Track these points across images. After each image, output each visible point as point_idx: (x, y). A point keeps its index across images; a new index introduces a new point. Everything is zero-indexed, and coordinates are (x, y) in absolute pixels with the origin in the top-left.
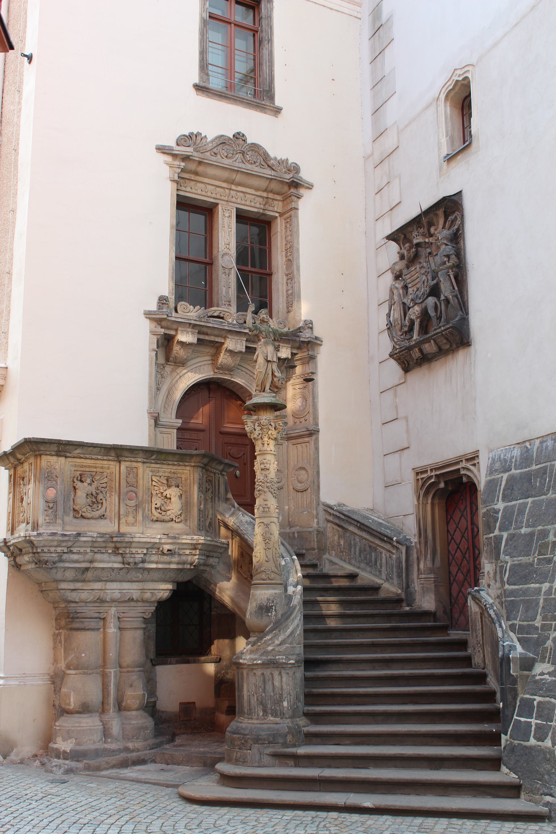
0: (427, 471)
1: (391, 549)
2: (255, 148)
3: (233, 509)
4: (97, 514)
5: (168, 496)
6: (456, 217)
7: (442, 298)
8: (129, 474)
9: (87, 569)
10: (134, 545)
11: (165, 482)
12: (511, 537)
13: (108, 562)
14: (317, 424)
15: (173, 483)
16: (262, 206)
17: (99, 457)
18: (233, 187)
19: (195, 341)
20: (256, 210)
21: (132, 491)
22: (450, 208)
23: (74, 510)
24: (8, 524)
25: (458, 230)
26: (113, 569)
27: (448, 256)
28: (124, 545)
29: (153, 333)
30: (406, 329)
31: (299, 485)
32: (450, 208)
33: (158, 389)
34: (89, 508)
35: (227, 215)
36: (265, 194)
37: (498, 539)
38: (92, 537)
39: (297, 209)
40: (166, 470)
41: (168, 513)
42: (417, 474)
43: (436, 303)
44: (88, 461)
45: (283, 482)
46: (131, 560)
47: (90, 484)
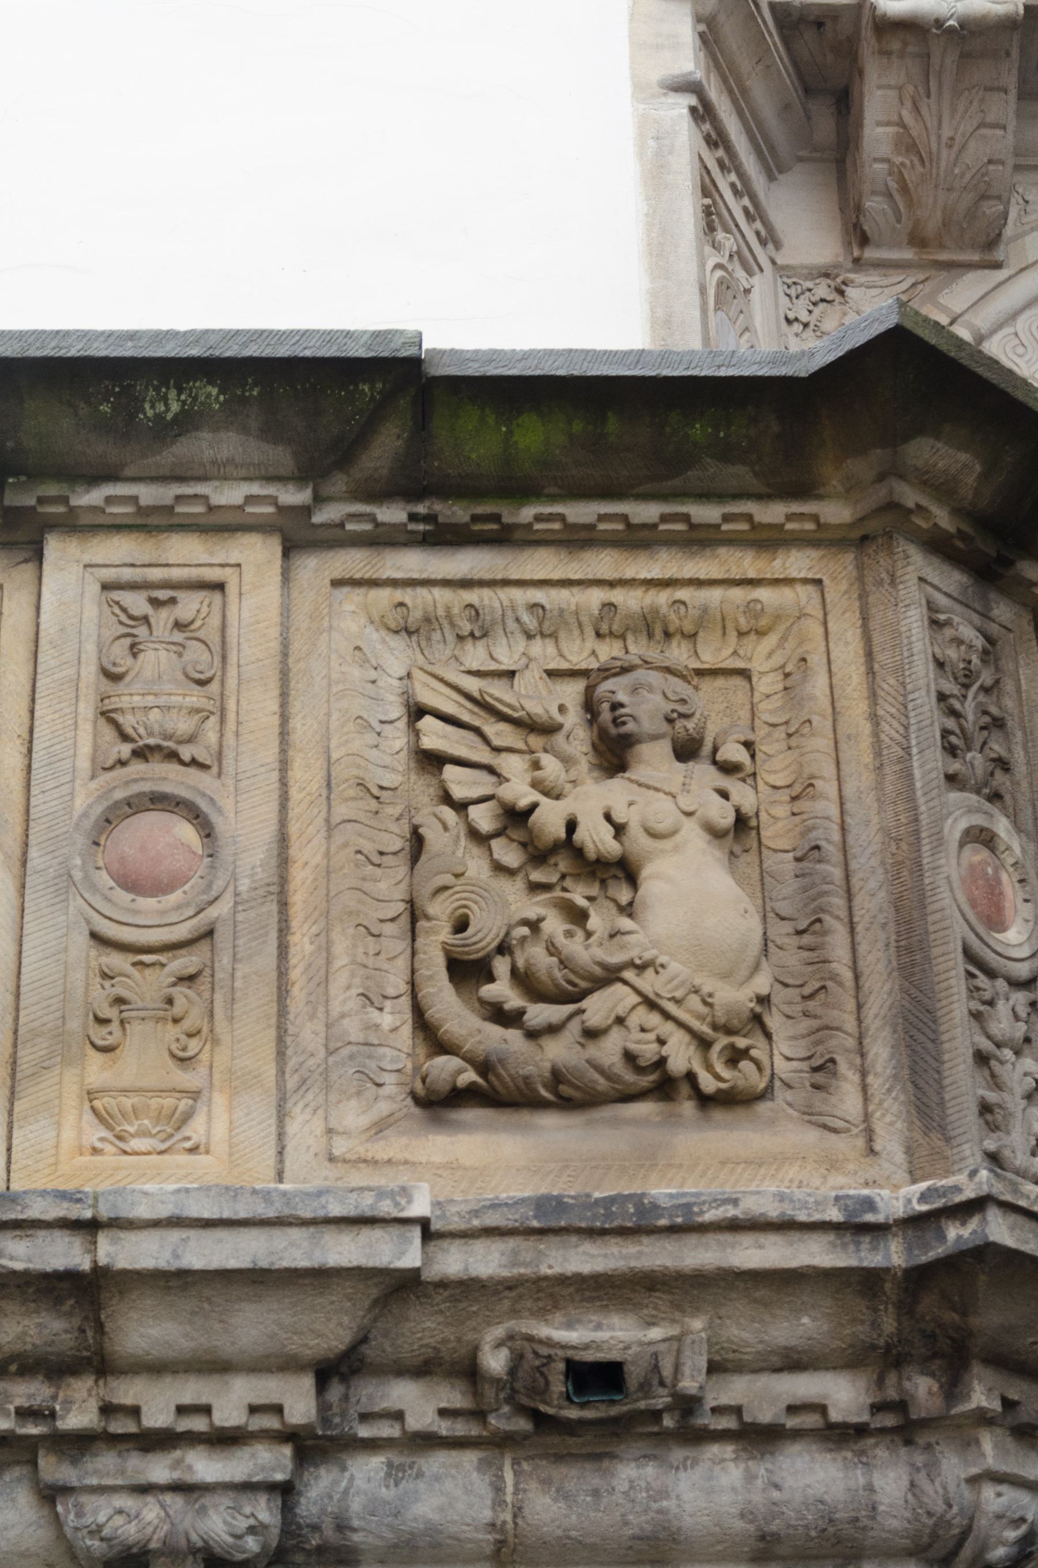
5: (597, 837)
8: (134, 650)
10: (143, 1329)
21: (160, 801)
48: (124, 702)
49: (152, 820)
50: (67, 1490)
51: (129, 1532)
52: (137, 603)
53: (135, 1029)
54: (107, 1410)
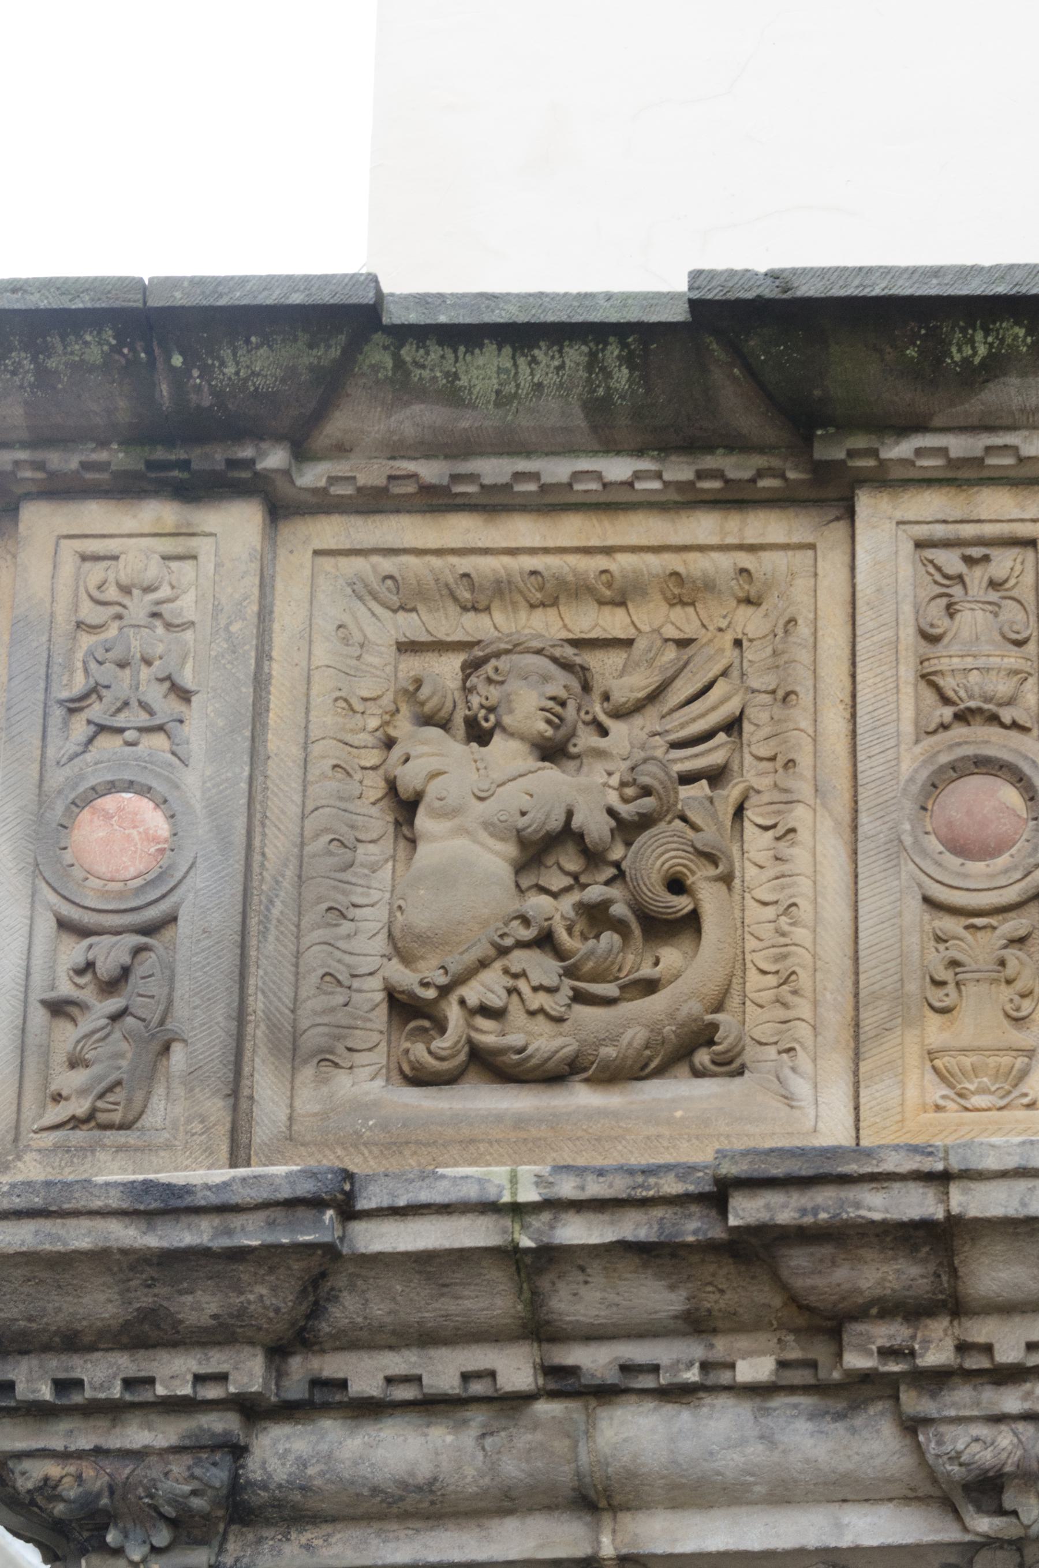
4: (629, 1025)
8: (951, 610)
10: (992, 1274)
17: (618, 469)
21: (984, 765)
28: (876, 1275)
38: (489, 1208)
44: (524, 530)
48: (944, 664)
49: (975, 784)
50: (927, 1421)
51: (986, 1457)
52: (951, 561)
53: (970, 990)
54: (963, 1348)
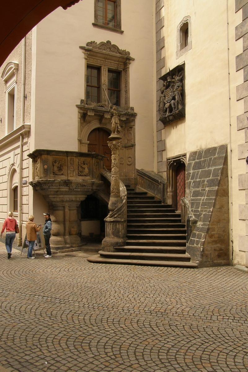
0: (170, 159)
1: (158, 185)
2: (114, 46)
3: (105, 171)
5: (84, 167)
6: (182, 73)
7: (176, 101)
9: (58, 191)
11: (83, 163)
12: (194, 182)
13: (64, 189)
14: (135, 143)
15: (85, 163)
16: (117, 67)
18: (107, 60)
19: (93, 115)
20: (114, 68)
22: (180, 70)
23: (53, 172)
24: (33, 177)
25: (182, 77)
26: (66, 191)
27: (179, 87)
29: (79, 112)
30: (164, 111)
31: (129, 163)
32: (180, 70)
33: (81, 131)
34: (58, 171)
35: (105, 70)
36: (118, 63)
37: (190, 182)
39: (129, 68)
40: (83, 159)
41: (84, 173)
42: (167, 160)
43: (174, 103)
45: (123, 162)
46: (72, 188)
47: (58, 164)
